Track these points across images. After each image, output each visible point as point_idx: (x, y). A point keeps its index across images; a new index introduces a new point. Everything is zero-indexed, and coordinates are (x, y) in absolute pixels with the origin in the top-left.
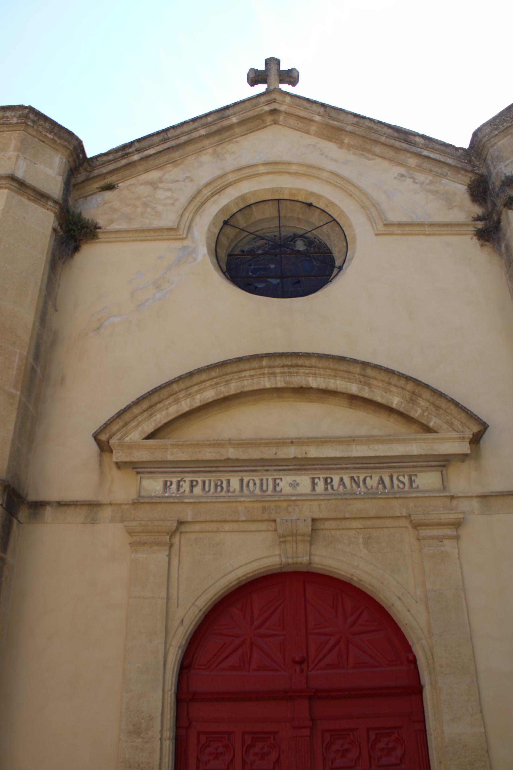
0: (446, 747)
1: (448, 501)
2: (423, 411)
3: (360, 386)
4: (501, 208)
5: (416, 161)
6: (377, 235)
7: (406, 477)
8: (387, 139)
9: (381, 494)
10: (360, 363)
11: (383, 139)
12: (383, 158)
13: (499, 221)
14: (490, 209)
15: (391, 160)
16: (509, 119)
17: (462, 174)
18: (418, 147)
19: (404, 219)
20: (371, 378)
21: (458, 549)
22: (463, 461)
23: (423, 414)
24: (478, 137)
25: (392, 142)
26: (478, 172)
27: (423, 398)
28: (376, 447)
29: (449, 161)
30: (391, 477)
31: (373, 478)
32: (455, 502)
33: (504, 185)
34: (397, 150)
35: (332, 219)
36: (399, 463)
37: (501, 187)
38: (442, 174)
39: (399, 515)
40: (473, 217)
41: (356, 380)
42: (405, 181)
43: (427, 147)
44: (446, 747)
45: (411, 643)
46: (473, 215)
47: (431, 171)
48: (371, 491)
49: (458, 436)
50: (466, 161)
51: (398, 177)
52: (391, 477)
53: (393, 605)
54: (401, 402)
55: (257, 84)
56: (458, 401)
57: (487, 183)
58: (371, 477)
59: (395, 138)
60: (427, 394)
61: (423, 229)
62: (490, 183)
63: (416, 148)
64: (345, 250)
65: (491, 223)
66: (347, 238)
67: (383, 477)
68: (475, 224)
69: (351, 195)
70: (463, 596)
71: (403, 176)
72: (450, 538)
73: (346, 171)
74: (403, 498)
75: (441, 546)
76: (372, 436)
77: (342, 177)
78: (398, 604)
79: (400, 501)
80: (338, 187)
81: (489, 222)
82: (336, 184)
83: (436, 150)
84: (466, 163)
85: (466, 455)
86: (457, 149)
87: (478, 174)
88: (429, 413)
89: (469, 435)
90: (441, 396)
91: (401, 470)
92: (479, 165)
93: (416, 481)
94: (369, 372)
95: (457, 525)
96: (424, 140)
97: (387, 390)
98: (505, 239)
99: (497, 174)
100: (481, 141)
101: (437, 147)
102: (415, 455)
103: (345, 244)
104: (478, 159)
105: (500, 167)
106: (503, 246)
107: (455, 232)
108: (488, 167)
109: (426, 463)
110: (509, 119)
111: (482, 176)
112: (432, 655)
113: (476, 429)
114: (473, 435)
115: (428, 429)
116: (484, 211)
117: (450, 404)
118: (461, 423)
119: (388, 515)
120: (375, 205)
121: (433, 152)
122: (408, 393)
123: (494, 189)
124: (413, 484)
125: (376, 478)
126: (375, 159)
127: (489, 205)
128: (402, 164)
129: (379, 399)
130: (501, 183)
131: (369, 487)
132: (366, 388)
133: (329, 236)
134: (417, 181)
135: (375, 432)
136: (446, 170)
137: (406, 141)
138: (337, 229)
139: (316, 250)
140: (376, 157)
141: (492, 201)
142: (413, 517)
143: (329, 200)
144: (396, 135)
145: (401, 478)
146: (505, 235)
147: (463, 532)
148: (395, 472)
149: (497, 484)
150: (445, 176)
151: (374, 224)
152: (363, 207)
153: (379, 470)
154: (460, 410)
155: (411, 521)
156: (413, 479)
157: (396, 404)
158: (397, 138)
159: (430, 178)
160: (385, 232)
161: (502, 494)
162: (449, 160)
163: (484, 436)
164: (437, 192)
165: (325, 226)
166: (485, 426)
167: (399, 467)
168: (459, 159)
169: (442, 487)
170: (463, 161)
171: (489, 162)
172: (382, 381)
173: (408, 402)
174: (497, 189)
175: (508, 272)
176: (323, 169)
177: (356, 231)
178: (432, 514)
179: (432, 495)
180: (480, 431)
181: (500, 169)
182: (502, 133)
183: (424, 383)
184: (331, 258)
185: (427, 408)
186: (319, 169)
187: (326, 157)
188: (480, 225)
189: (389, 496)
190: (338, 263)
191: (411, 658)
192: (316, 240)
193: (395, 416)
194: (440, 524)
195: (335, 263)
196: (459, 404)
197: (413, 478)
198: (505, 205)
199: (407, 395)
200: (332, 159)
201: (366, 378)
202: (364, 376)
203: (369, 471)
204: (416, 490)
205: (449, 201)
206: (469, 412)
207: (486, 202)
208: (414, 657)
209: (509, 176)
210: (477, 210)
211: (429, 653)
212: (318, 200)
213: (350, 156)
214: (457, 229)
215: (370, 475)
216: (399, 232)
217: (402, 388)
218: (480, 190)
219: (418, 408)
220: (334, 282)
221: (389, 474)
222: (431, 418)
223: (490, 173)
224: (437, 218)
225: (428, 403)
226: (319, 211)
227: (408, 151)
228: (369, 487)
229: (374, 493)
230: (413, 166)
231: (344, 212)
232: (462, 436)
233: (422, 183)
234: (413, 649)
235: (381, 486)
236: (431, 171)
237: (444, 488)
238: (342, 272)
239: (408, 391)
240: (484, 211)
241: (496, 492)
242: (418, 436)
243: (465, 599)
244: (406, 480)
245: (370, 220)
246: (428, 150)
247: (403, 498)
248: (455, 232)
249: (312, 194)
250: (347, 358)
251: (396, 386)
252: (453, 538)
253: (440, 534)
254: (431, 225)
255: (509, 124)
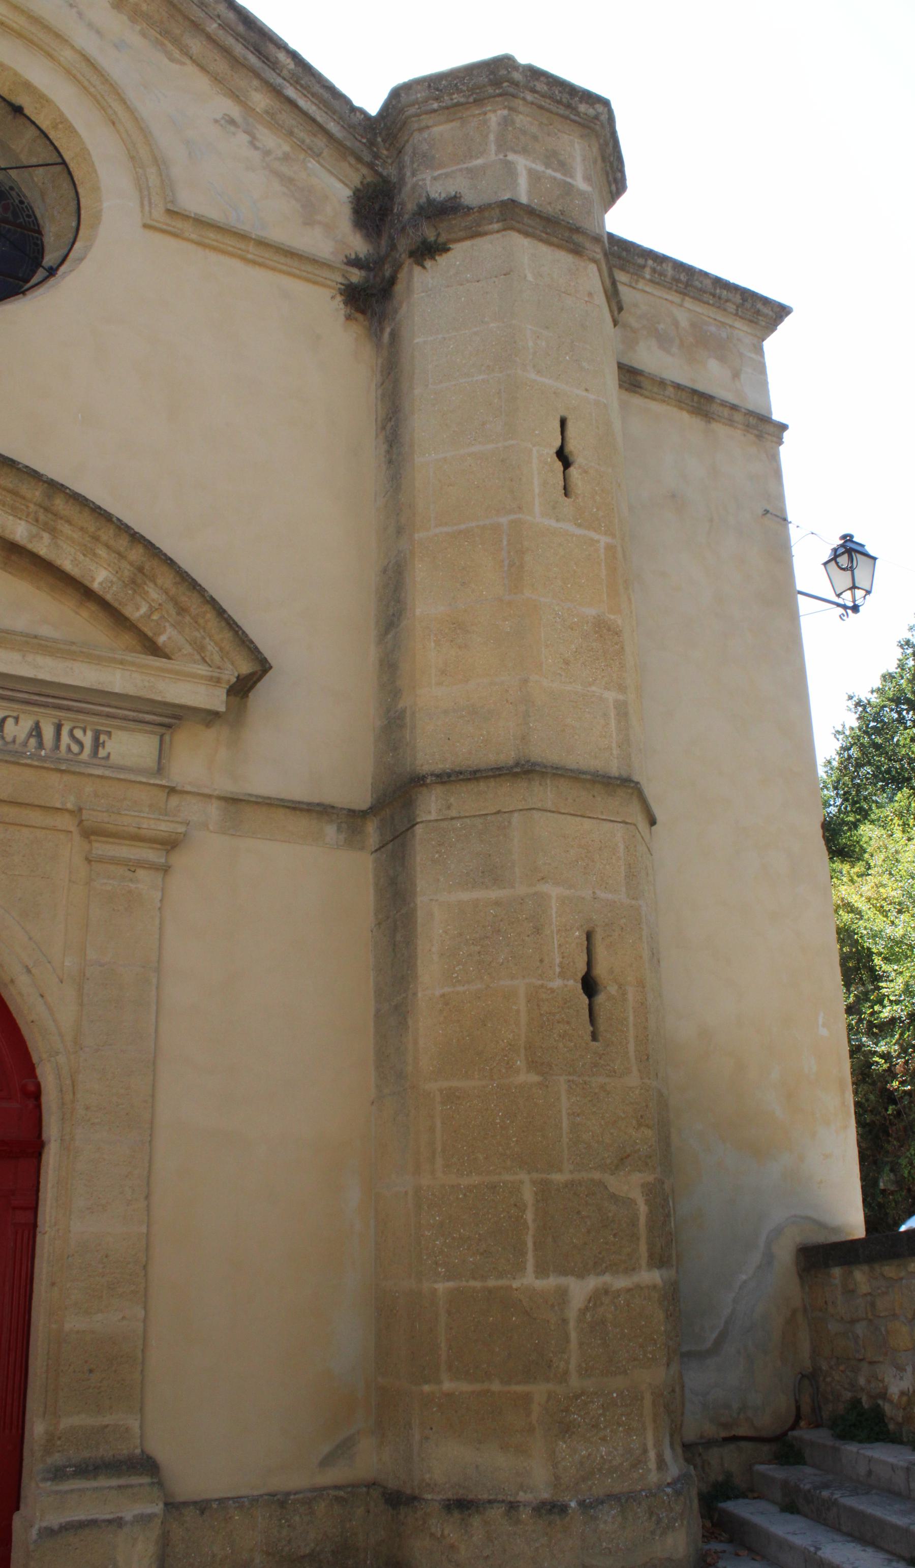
0: (68, 1257)
1: (163, 795)
2: (152, 610)
3: (34, 530)
4: (403, 256)
5: (268, 101)
6: (146, 226)
7: (89, 734)
8: (221, 32)
9: (31, 757)
10: (45, 482)
11: (212, 27)
12: (203, 68)
13: (392, 281)
14: (383, 251)
15: (216, 79)
16: (465, 88)
17: (350, 164)
18: (279, 75)
19: (212, 213)
20: (61, 518)
21: (163, 890)
22: (208, 725)
23: (149, 616)
24: (399, 102)
25: (230, 41)
26: (380, 169)
27: (156, 584)
28: (40, 660)
29: (332, 127)
30: (58, 728)
31: (20, 721)
32: (174, 801)
33: (420, 214)
34: (236, 63)
35: (60, 160)
36: (80, 701)
37: (414, 215)
38: (311, 149)
39: (58, 805)
40: (346, 257)
41: (28, 515)
42: (234, 134)
43: (295, 81)
44: (68, 1257)
45: (35, 1059)
46: (347, 252)
47: (291, 133)
48: (11, 747)
49: (209, 674)
50: (364, 141)
51: (223, 122)
52: (58, 728)
53: (12, 981)
54: (112, 582)
55: (780, 442)
56: (225, 606)
57: (391, 199)
58: (17, 719)
59: (237, 36)
60: (167, 579)
61: (243, 246)
62: (397, 200)
63: (275, 75)
64: (71, 236)
65: (378, 279)
66: (82, 212)
67: (42, 725)
68: (347, 272)
69: (114, 123)
70: (154, 981)
71: (232, 122)
72: (150, 868)
73: (115, 65)
74: (74, 773)
75: (131, 880)
76: (36, 637)
77: (103, 75)
78: (23, 980)
79: (66, 778)
80: (90, 93)
81: (375, 277)
82: (86, 83)
83: (313, 95)
84: (364, 144)
85: (216, 714)
86: (354, 109)
87: (380, 175)
88: (162, 617)
89: (230, 676)
90: (194, 588)
91: (81, 717)
92: (387, 157)
93: (107, 744)
94: (59, 503)
95: (171, 844)
96: (295, 65)
97: (89, 552)
98: (394, 319)
99: (415, 186)
100: (402, 111)
101: (317, 88)
102: (116, 694)
103: (74, 224)
104: (387, 145)
105: (424, 176)
106: (388, 330)
107: (304, 274)
108: (401, 169)
109: (131, 714)
110: (465, 88)
111: (385, 180)
112: (73, 1086)
113: (246, 667)
114: (238, 678)
115: (153, 648)
116: (371, 251)
117: (207, 608)
118: (221, 649)
119: (36, 803)
120: (160, 163)
121: (305, 96)
122: (128, 567)
123: (400, 215)
124: (100, 749)
125: (26, 724)
126: (183, 64)
127: (383, 243)
128: (237, 96)
129: (67, 566)
130: (415, 208)
131: (9, 738)
132: (46, 536)
133: (43, 195)
134: (258, 144)
135: (45, 631)
136: (320, 142)
137: (259, 52)
138: (66, 185)
139: (9, 215)
140: (188, 61)
141: (391, 238)
142: (85, 815)
143: (62, 115)
144: (241, 28)
145: (78, 733)
146: (396, 311)
147: (180, 860)
148: (68, 719)
149: (262, 781)
150: (317, 155)
151: (146, 203)
152: (132, 158)
153: (36, 709)
154: (223, 624)
155: (81, 822)
156: (101, 741)
157: (101, 584)
158: (242, 38)
159: (286, 148)
160: (165, 227)
161: (268, 801)
162: (332, 124)
163: (259, 685)
164: (291, 180)
165: (41, 169)
166: (264, 667)
167: (80, 711)
168: (351, 130)
169: (155, 766)
170: (359, 138)
171: (407, 159)
172: (82, 529)
173: (126, 586)
174: (406, 217)
175: (382, 384)
176: (67, 41)
177: (105, 205)
178: (127, 815)
179: (132, 777)
180: (252, 674)
181: (424, 180)
182: (446, 112)
183: (165, 555)
184: (36, 244)
185: (160, 605)
186: (58, 36)
187: (80, 15)
188: (356, 276)
189: (46, 765)
190: (49, 259)
191: (31, 1088)
192: (13, 193)
193: (93, 607)
194: (137, 838)
195: (43, 258)
196: (224, 611)
197: (103, 738)
198: (412, 254)
199: (127, 571)
200: (90, 25)
201: (50, 516)
202: (46, 510)
203: (15, 706)
204: (103, 762)
205: (309, 207)
206: (240, 632)
207: (379, 234)
208: (38, 1086)
209: (434, 200)
210: (359, 245)
211: (68, 1082)
212: (38, 106)
213: (133, 36)
214: (309, 268)
215: (15, 714)
216: (194, 236)
217: (119, 554)
218: (374, 207)
219: (144, 603)
220: (30, 295)
221: (56, 721)
222: (165, 627)
223: (402, 179)
224: (277, 235)
225: (164, 597)
226: (31, 132)
227: (257, 75)
228: (9, 738)
229: (17, 752)
230: (258, 110)
231: (89, 154)
232: (215, 674)
233: (267, 153)
234: (38, 1071)
235: (33, 741)
236: (291, 133)
237: (160, 769)
238: (52, 281)
239: (131, 564)
240: (371, 251)
241: (257, 796)
242: (130, 657)
243: (157, 988)
244: (88, 740)
245: (141, 191)
246: (296, 89)
247: (74, 773)
248: (304, 274)
249: (28, 86)
250: (19, 463)
251: (108, 547)
252: (157, 869)
253: (132, 857)
254: (262, 244)
255: (462, 100)
